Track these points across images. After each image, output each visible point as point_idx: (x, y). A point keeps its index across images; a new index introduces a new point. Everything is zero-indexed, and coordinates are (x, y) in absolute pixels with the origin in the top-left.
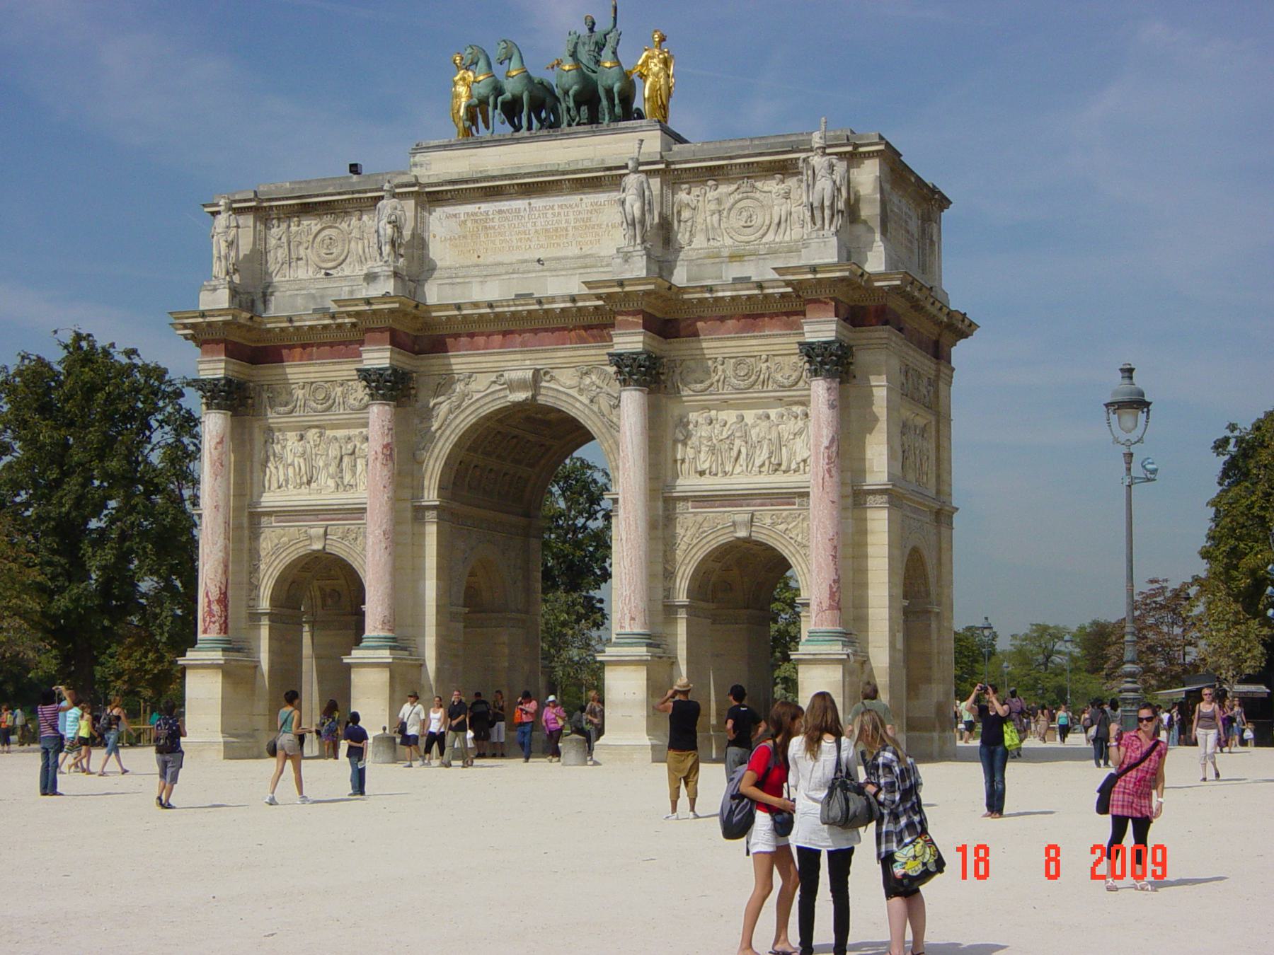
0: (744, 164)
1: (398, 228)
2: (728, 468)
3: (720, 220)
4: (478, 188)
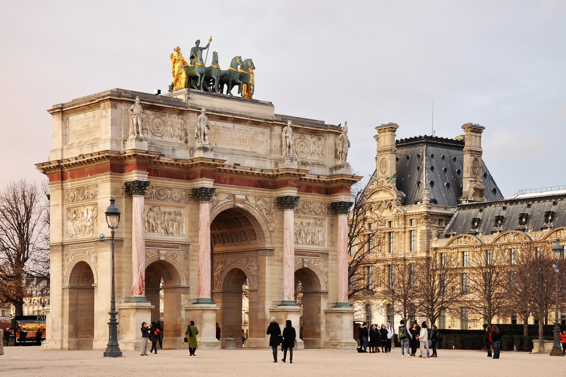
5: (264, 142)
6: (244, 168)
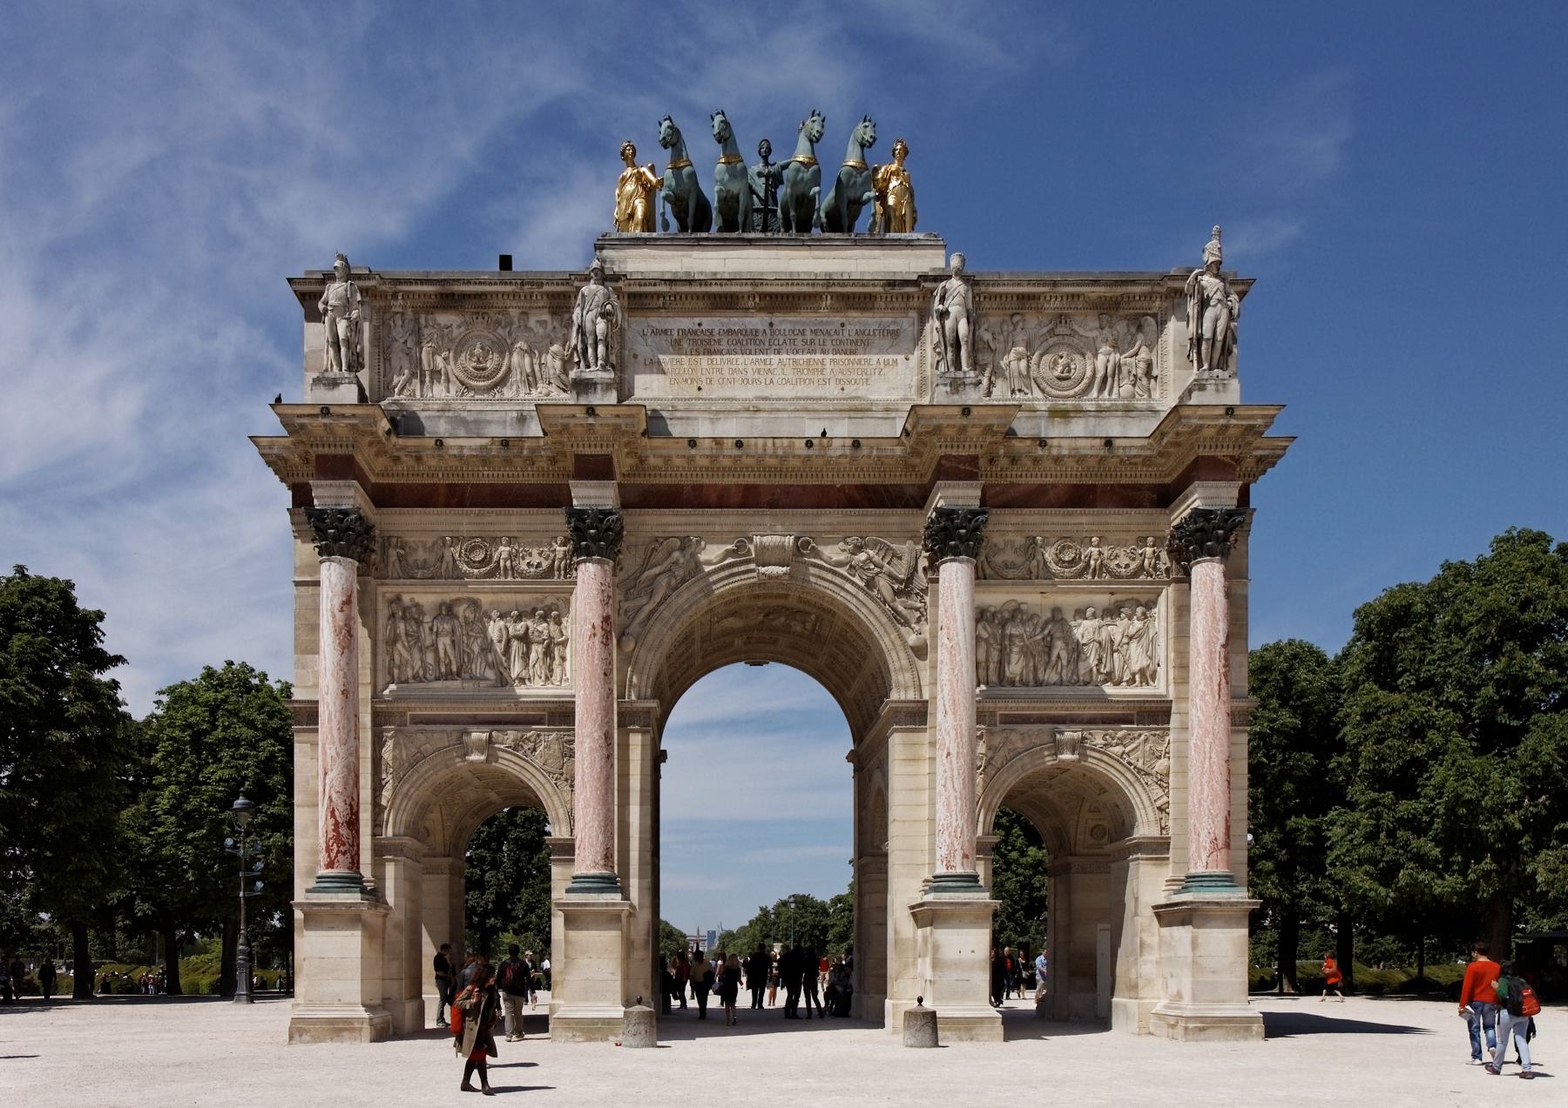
2: (1040, 676)
3: (1028, 367)
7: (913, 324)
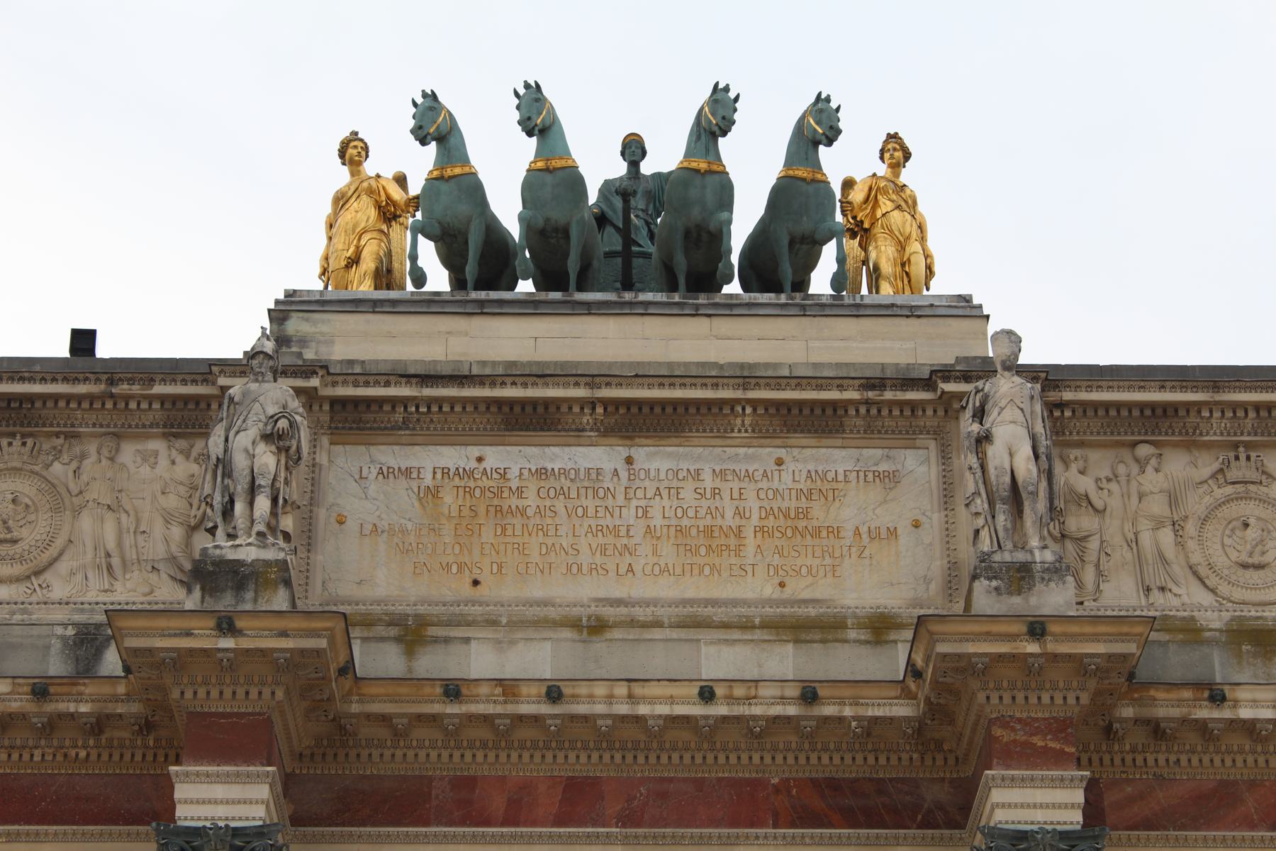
0: (1244, 406)
1: (288, 457)
3: (1180, 543)
4: (490, 402)
5: (893, 533)
6: (638, 690)
7: (928, 459)
